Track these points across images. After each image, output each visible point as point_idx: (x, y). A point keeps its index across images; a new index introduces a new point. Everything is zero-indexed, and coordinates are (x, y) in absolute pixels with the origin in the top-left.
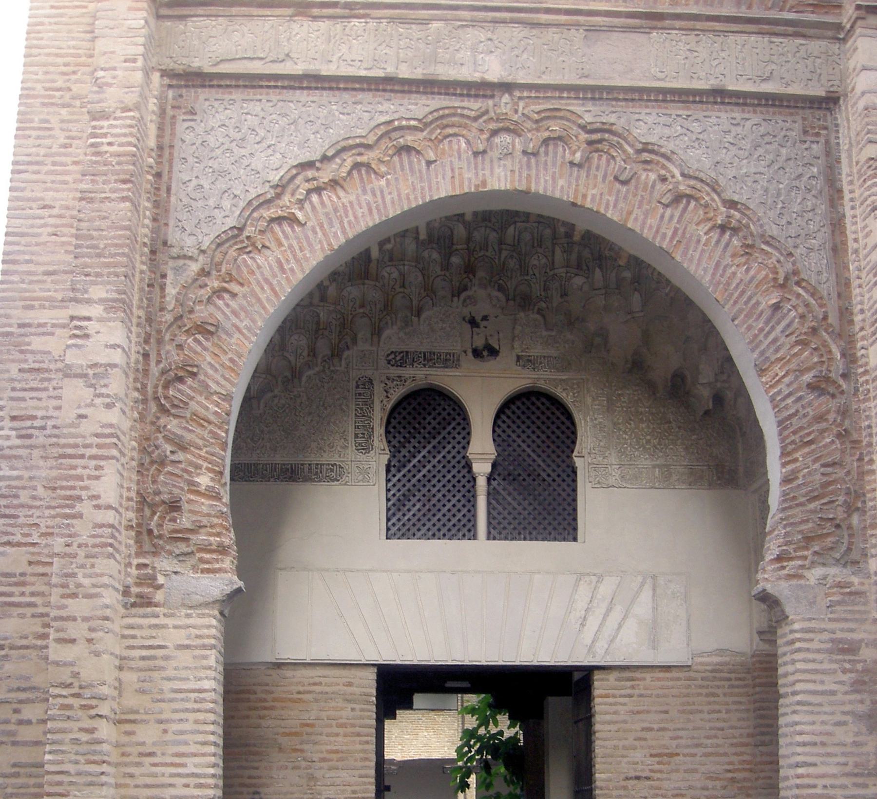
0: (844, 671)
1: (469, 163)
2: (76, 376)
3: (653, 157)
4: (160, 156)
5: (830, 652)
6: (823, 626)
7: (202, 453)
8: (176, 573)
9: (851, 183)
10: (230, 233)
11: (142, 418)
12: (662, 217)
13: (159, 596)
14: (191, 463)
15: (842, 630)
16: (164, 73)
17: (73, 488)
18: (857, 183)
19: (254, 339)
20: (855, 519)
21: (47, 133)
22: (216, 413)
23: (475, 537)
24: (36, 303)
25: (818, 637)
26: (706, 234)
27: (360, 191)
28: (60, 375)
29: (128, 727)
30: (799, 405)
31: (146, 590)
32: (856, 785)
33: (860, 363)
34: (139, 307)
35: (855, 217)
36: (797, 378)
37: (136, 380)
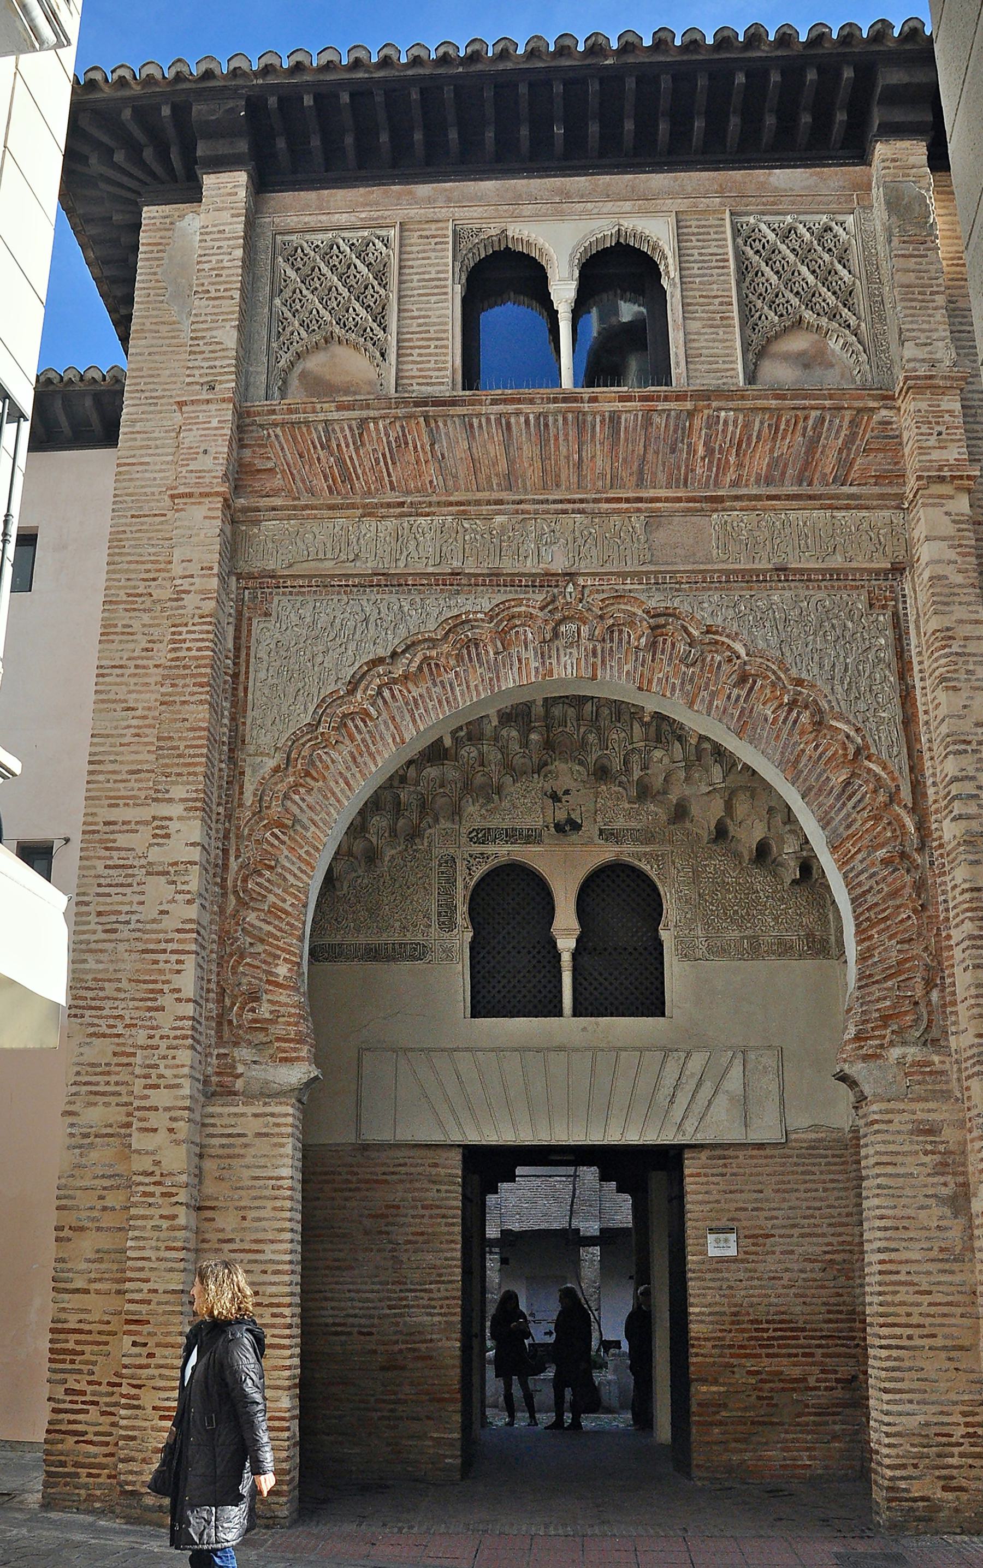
0: (926, 1153)
1: (536, 653)
2: (158, 874)
3: (717, 637)
4: (237, 657)
5: (912, 1133)
6: (901, 1106)
9: (920, 653)
11: (222, 911)
12: (729, 697)
15: (923, 1111)
16: (239, 577)
17: (155, 982)
18: (926, 655)
19: (330, 832)
20: (935, 995)
21: (131, 638)
22: (292, 905)
23: (560, 1014)
24: (121, 802)
25: (897, 1118)
27: (430, 684)
28: (144, 870)
30: (872, 882)
32: (945, 1271)
33: (935, 836)
34: (219, 804)
35: (923, 688)
36: (869, 855)
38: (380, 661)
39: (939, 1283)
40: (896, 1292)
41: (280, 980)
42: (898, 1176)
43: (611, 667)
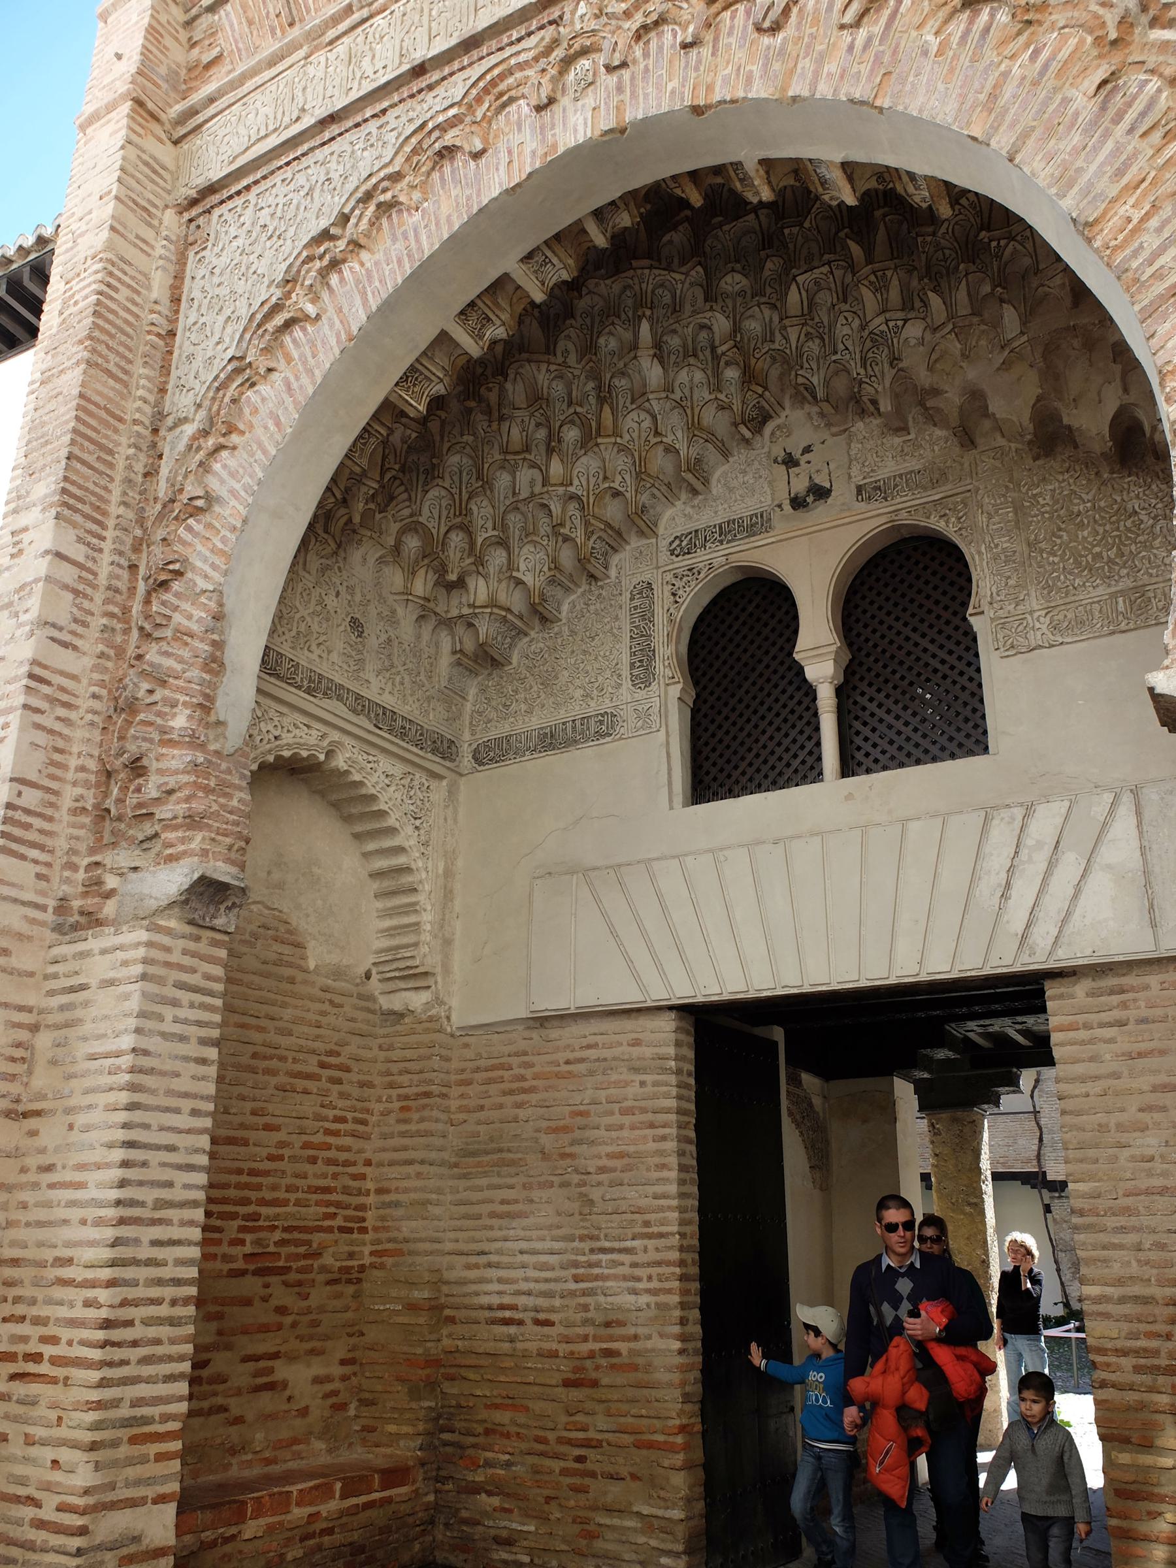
7: (180, 683)
8: (135, 869)
10: (229, 368)
12: (851, 48)
14: (165, 700)
16: (182, 209)
26: (937, 33)
27: (389, 242)
29: (32, 1123)
37: (107, 601)
38: (325, 235)
41: (175, 736)
43: (646, 96)
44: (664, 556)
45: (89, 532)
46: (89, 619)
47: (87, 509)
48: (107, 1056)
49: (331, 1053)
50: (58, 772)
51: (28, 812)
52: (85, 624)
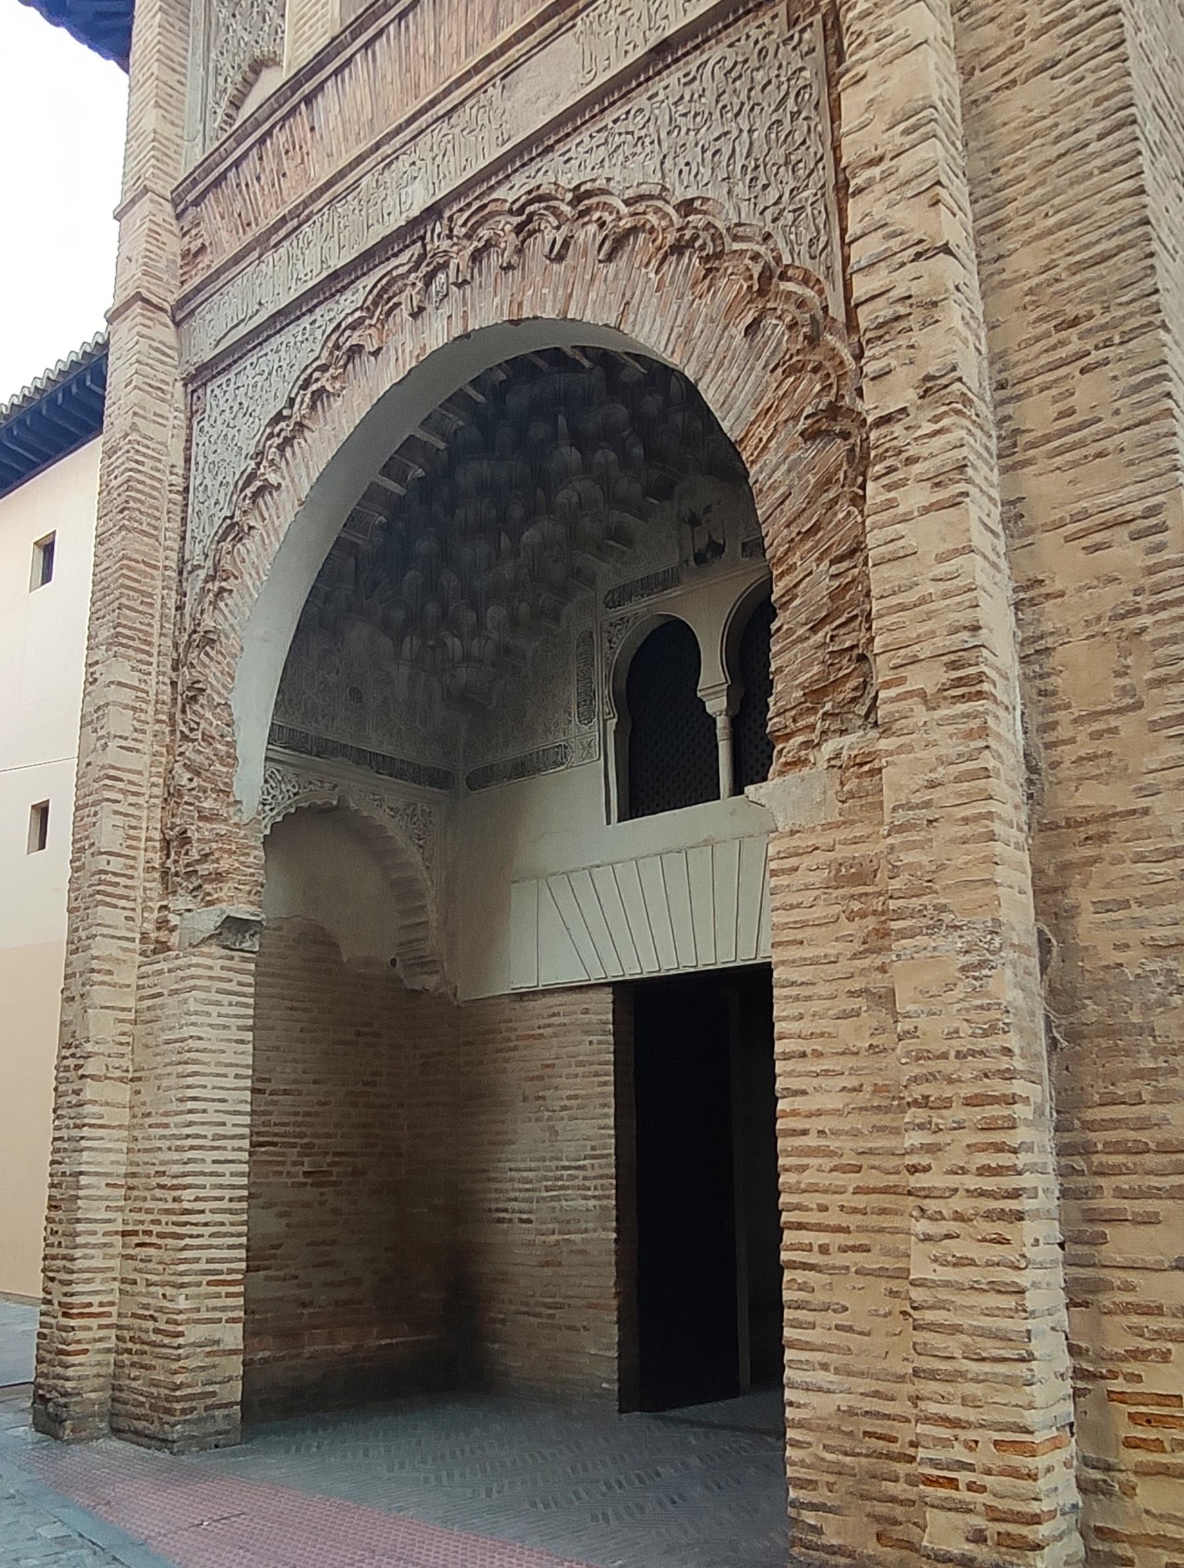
8: (189, 910)
13: (174, 939)
31: (163, 935)
32: (881, 1129)
37: (157, 712)
39: (871, 1152)
40: (803, 1168)
42: (804, 962)
44: (601, 606)
45: (140, 661)
46: (146, 727)
47: (136, 644)
48: (176, 1041)
49: (366, 1025)
50: (134, 843)
51: (115, 874)
52: (143, 732)
